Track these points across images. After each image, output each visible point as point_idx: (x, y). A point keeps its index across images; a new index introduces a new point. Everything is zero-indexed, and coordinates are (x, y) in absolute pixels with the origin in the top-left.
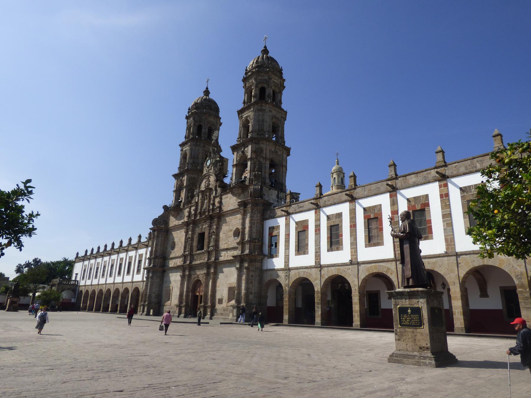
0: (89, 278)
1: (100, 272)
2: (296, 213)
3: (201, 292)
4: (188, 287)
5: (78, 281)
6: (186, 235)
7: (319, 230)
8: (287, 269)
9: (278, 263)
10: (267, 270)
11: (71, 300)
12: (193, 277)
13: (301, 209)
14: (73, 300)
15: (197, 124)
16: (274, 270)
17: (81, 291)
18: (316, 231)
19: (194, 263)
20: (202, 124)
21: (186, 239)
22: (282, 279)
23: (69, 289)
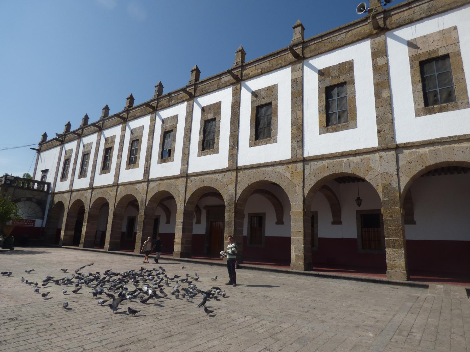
0: (83, 174)
1: (120, 157)
5: (49, 184)
11: (34, 221)
14: (38, 223)
17: (61, 204)
23: (29, 199)
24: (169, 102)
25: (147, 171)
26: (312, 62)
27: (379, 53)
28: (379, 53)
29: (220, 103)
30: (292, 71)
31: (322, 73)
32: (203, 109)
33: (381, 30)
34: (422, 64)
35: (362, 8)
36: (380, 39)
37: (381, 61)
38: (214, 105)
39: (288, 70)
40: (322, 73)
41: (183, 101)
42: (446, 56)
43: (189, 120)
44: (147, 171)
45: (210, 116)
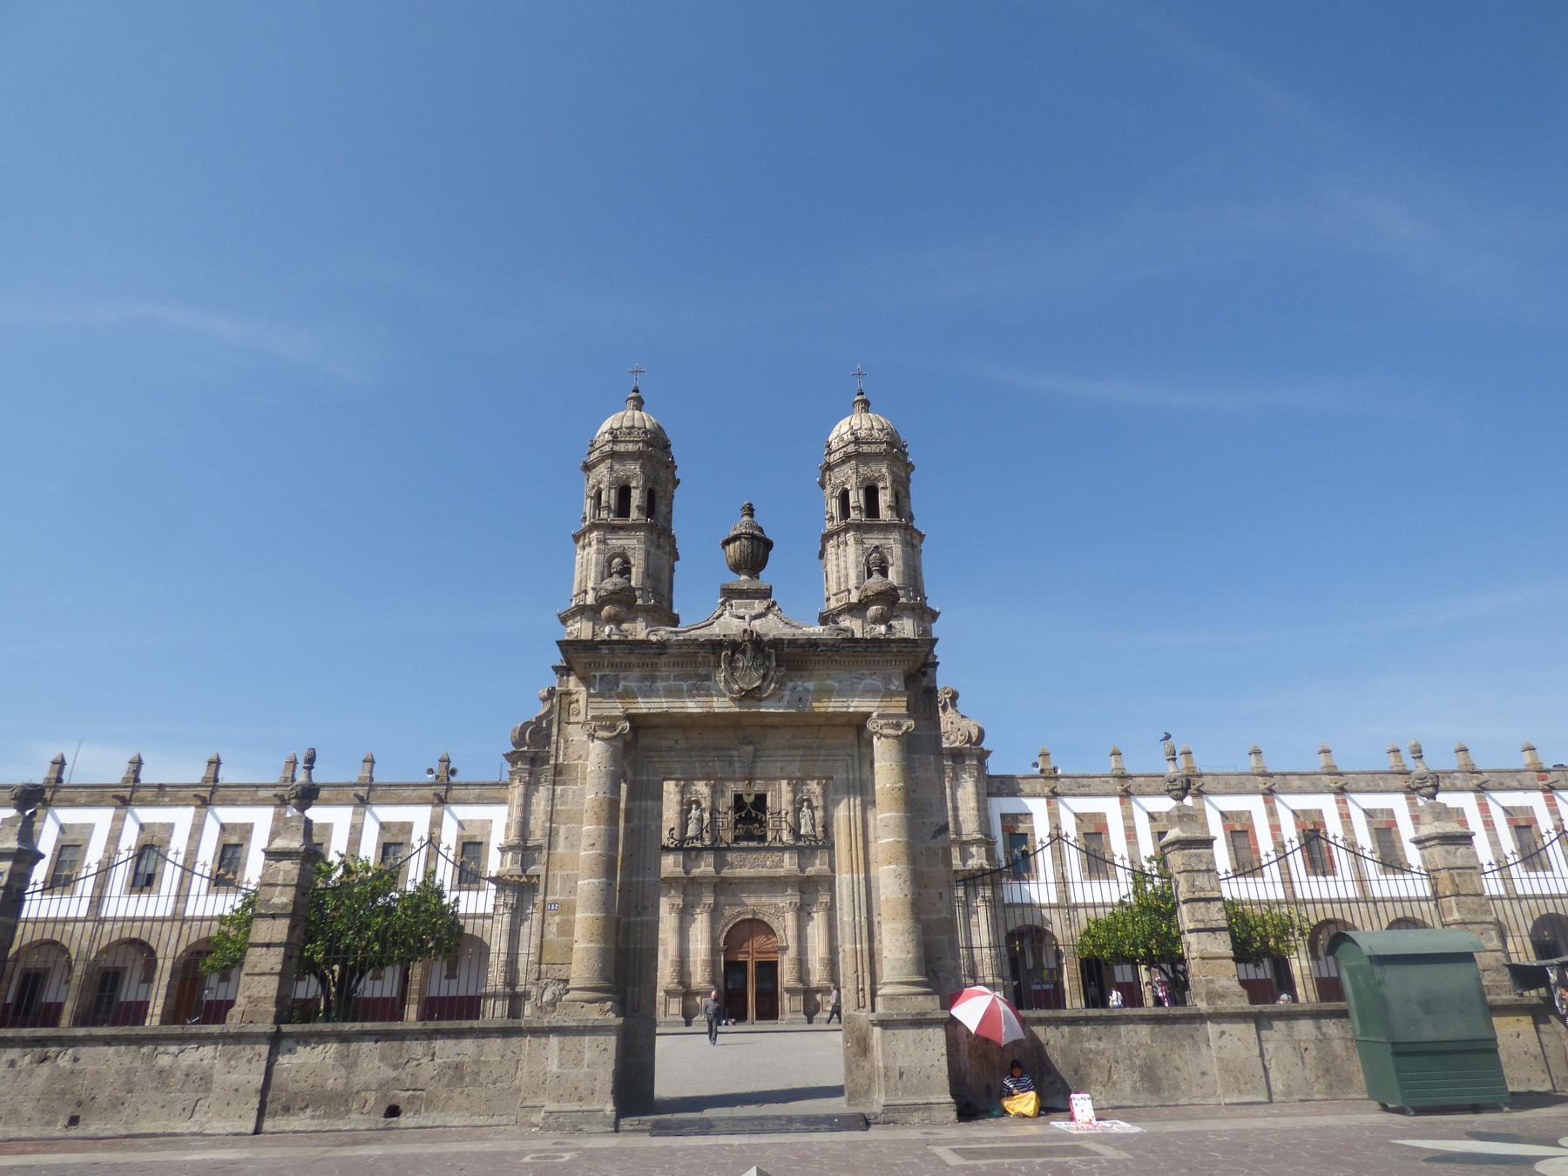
2: (1074, 795)
3: (750, 955)
4: (714, 940)
6: (682, 792)
7: (1135, 836)
8: (1066, 906)
9: (1040, 890)
10: (1012, 905)
12: (728, 911)
13: (1083, 790)
15: (649, 485)
16: (1032, 905)
18: (1128, 837)
19: (726, 872)
20: (658, 488)
21: (681, 803)
22: (1057, 926)
24: (157, 796)
25: (97, 901)
26: (375, 809)
27: (436, 823)
28: (436, 823)
29: (252, 825)
30: (354, 813)
31: (384, 827)
32: (223, 827)
33: (441, 801)
34: (465, 845)
35: (431, 771)
36: (439, 809)
37: (436, 830)
38: (243, 825)
39: (350, 810)
40: (384, 827)
41: (188, 805)
42: (480, 843)
43: (196, 836)
44: (97, 901)
45: (234, 840)
